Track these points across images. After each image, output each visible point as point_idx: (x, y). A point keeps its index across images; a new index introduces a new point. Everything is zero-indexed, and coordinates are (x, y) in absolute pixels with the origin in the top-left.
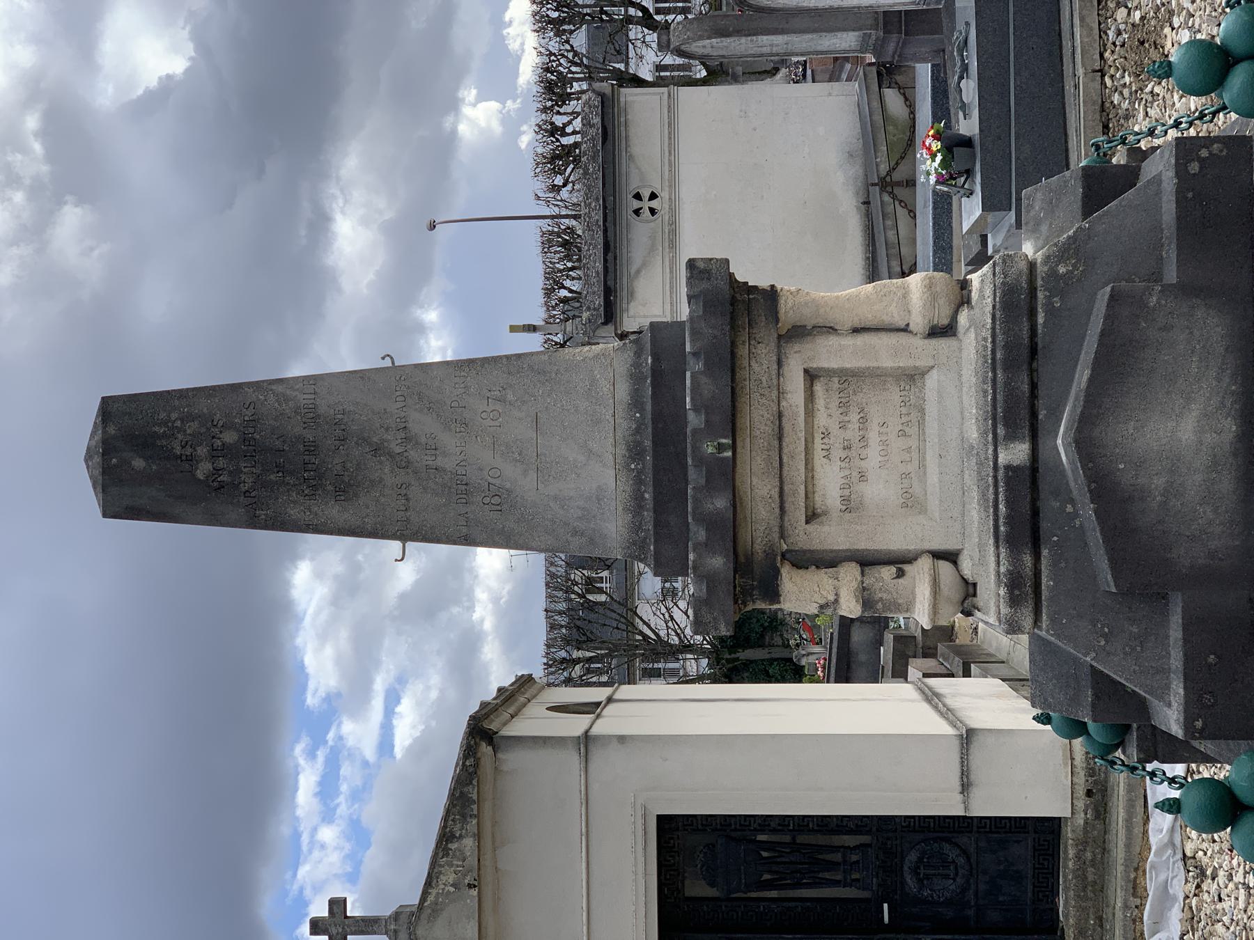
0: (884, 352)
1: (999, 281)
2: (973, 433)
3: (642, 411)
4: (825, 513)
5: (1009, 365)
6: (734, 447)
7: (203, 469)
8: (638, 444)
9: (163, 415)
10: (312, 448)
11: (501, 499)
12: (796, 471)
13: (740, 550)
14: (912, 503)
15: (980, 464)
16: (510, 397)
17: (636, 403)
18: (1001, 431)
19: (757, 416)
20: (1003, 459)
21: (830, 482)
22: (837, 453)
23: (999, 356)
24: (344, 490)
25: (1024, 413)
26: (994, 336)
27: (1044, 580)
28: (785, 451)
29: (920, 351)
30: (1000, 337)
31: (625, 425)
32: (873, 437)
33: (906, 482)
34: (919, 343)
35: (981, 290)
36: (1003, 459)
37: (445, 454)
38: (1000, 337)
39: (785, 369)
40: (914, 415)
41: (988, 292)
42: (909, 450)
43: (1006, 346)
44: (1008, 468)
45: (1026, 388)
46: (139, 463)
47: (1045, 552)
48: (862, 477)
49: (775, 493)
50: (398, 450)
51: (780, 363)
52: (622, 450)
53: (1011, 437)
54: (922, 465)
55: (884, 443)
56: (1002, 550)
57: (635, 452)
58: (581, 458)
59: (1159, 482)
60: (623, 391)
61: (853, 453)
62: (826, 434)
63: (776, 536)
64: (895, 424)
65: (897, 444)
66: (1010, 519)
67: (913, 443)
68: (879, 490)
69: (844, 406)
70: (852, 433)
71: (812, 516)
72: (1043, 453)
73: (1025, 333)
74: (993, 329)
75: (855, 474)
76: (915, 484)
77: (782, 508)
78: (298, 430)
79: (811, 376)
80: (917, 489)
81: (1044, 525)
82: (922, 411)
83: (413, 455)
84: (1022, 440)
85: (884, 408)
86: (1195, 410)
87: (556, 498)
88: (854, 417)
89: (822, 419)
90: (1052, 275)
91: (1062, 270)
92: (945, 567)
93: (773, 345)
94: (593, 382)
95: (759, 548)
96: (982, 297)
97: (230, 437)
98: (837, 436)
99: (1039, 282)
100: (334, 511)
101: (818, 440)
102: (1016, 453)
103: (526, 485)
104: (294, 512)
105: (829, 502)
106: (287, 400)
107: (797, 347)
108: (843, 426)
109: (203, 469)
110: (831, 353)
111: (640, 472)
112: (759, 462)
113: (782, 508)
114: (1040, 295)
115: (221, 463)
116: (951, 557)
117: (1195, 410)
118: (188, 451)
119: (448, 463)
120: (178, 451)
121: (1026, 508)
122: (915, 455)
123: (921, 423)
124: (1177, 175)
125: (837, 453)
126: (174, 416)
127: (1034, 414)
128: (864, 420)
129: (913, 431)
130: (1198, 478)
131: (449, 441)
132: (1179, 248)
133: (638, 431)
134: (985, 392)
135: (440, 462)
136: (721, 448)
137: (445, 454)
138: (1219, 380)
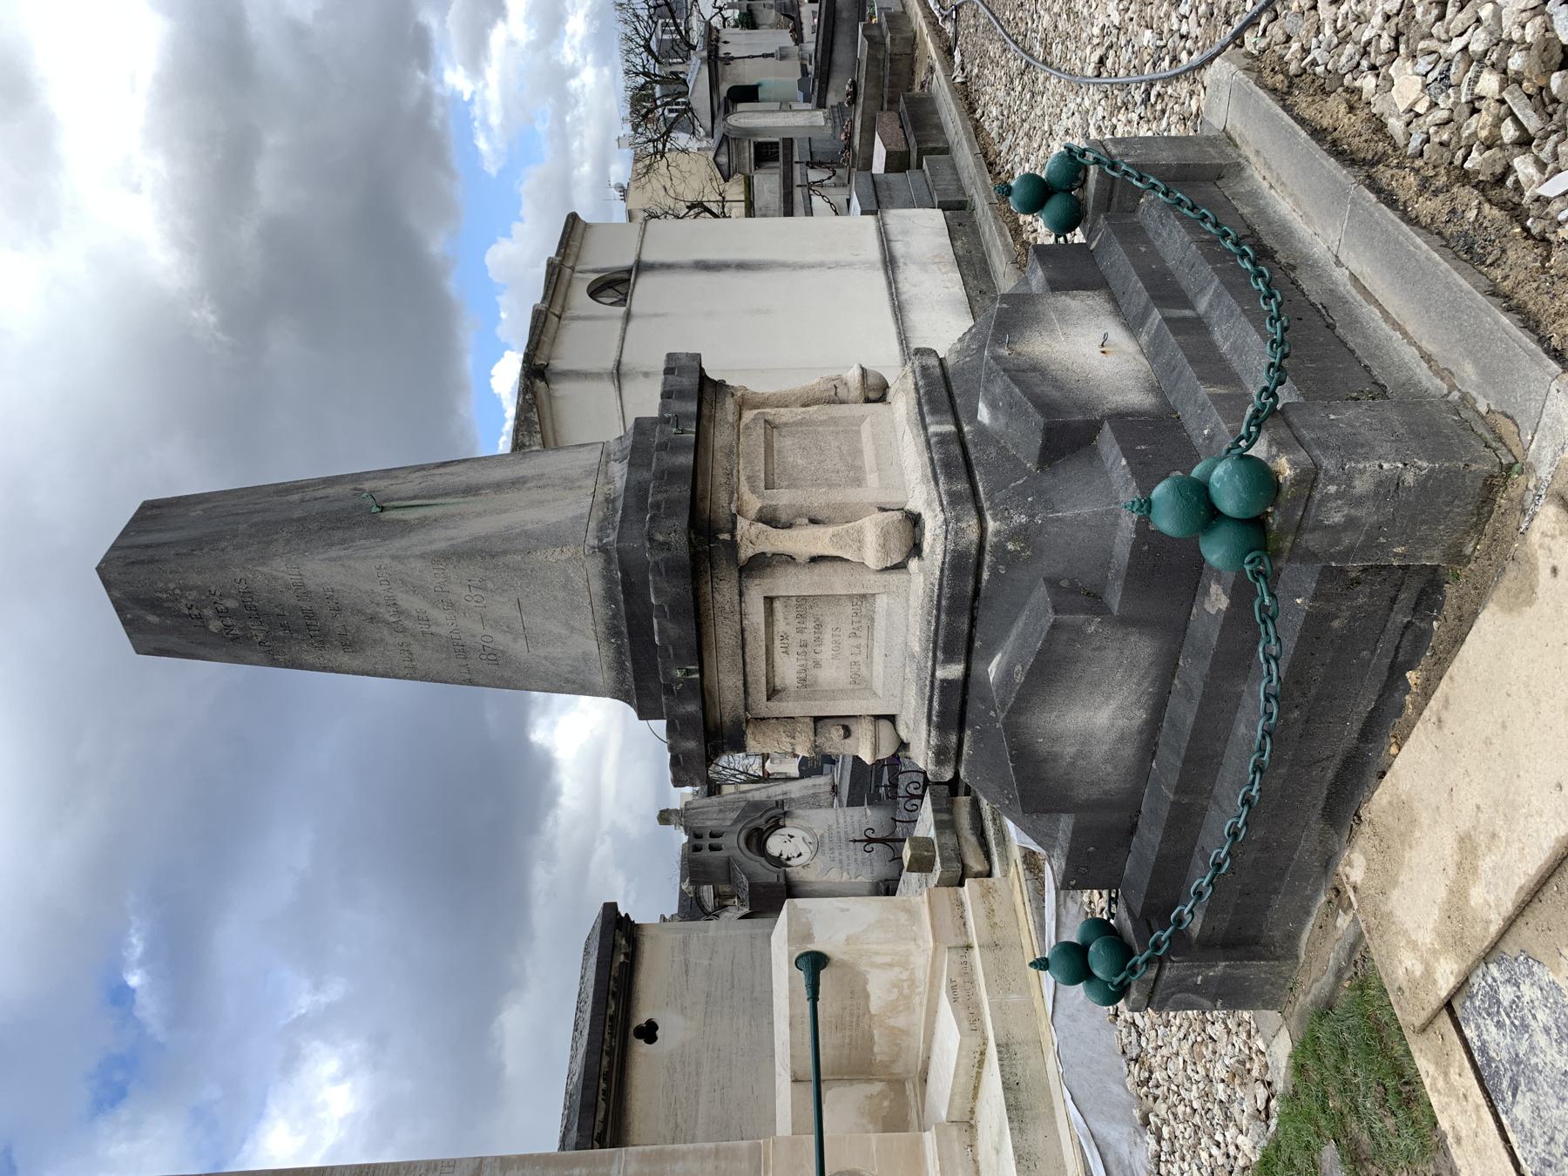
0: (836, 582)
1: (951, 547)
2: (917, 648)
3: (616, 602)
4: (784, 689)
5: (952, 611)
6: (701, 671)
7: (215, 625)
8: (615, 627)
9: (161, 585)
10: (310, 615)
11: (495, 656)
12: (758, 668)
13: (711, 724)
14: (859, 683)
15: (920, 669)
16: (490, 585)
17: (610, 597)
18: (940, 655)
19: (724, 633)
20: (940, 674)
21: (788, 670)
22: (795, 648)
23: (944, 603)
24: (349, 644)
25: (962, 644)
26: (941, 585)
27: (965, 748)
28: (748, 654)
29: (872, 583)
30: (946, 590)
31: (602, 611)
32: (827, 637)
33: (855, 668)
34: (873, 577)
35: (932, 547)
36: (940, 674)
37: (437, 624)
38: (946, 590)
39: (746, 598)
40: (865, 622)
41: (939, 549)
42: (858, 647)
43: (952, 598)
44: (942, 681)
45: (966, 627)
46: (153, 619)
47: (968, 732)
48: (817, 664)
49: (740, 684)
50: (392, 619)
51: (741, 594)
52: (601, 628)
53: (949, 660)
54: (869, 656)
55: (837, 644)
56: (933, 733)
57: (613, 631)
58: (564, 632)
59: (1071, 750)
60: (597, 586)
61: (809, 649)
62: (784, 637)
63: (741, 711)
64: (847, 629)
65: (847, 643)
66: (941, 714)
67: (863, 642)
68: (831, 672)
69: (801, 617)
70: (809, 636)
71: (773, 693)
72: (973, 672)
73: (970, 588)
74: (941, 580)
75: (810, 663)
76: (863, 668)
77: (746, 692)
78: (293, 601)
79: (769, 600)
80: (864, 671)
81: (970, 716)
82: (872, 620)
83: (407, 623)
84: (959, 662)
85: (838, 622)
86: (1113, 705)
87: (546, 658)
88: (810, 624)
89: (780, 626)
90: (999, 548)
91: (1010, 546)
92: (885, 726)
93: (734, 582)
94: (568, 579)
95: (726, 719)
96: (933, 552)
97: (231, 604)
98: (795, 639)
99: (988, 548)
100: (344, 659)
101: (777, 643)
102: (955, 671)
103: (518, 648)
104: (309, 658)
105: (787, 682)
106: (275, 579)
107: (757, 581)
108: (800, 631)
109: (215, 625)
110: (786, 584)
111: (619, 647)
112: (725, 664)
113: (746, 692)
114: (988, 558)
115: (229, 621)
116: (892, 719)
117: (1113, 705)
118: (196, 612)
119: (444, 631)
120: (186, 611)
121: (956, 707)
122: (864, 651)
123: (870, 628)
124: (1137, 532)
125: (795, 648)
126: (172, 586)
127: (971, 640)
128: (819, 626)
129: (864, 633)
130: (1105, 747)
131: (437, 614)
132: (1125, 589)
133: (614, 617)
134: (929, 622)
135: (433, 629)
136: (688, 672)
137: (437, 624)
138: (1139, 684)
